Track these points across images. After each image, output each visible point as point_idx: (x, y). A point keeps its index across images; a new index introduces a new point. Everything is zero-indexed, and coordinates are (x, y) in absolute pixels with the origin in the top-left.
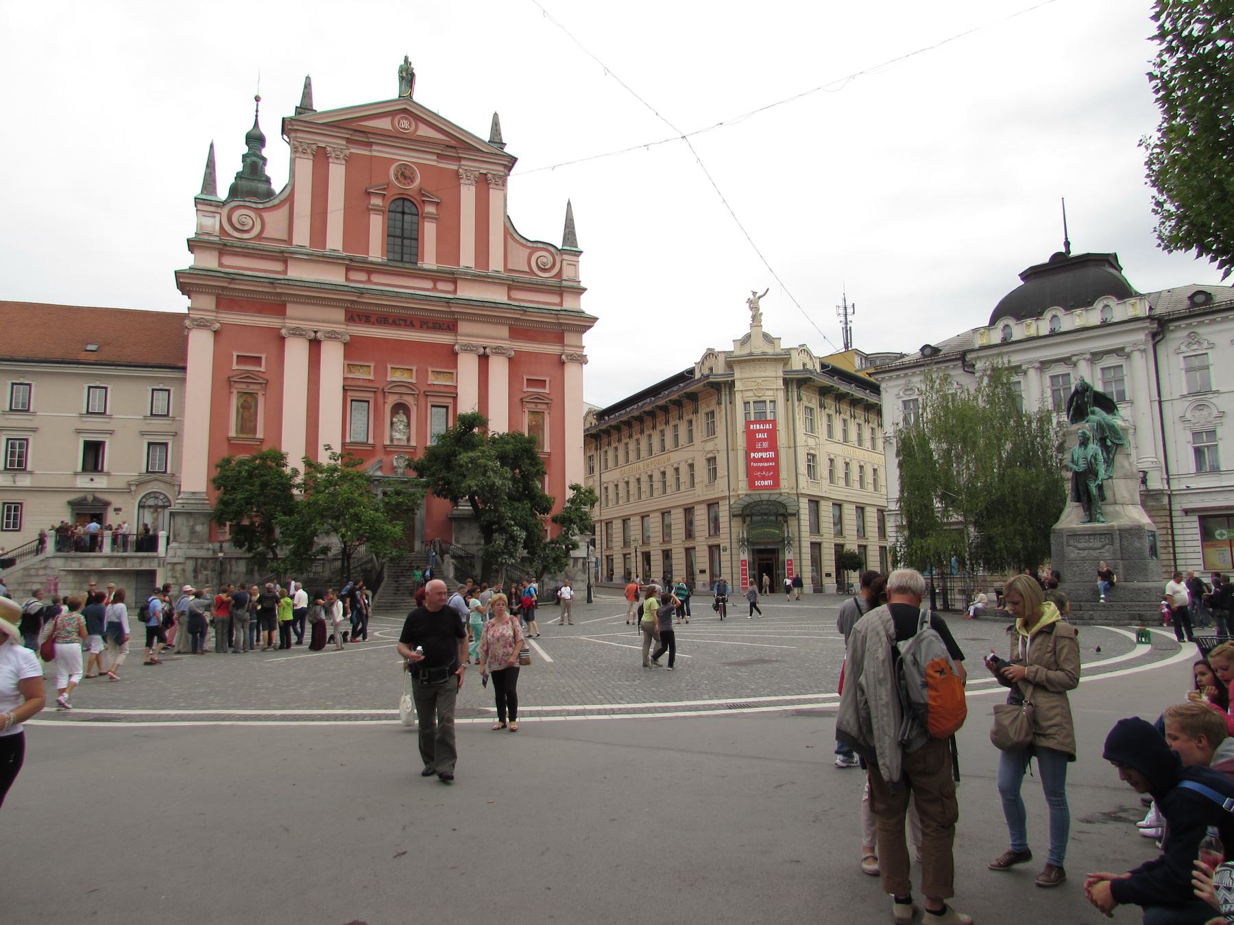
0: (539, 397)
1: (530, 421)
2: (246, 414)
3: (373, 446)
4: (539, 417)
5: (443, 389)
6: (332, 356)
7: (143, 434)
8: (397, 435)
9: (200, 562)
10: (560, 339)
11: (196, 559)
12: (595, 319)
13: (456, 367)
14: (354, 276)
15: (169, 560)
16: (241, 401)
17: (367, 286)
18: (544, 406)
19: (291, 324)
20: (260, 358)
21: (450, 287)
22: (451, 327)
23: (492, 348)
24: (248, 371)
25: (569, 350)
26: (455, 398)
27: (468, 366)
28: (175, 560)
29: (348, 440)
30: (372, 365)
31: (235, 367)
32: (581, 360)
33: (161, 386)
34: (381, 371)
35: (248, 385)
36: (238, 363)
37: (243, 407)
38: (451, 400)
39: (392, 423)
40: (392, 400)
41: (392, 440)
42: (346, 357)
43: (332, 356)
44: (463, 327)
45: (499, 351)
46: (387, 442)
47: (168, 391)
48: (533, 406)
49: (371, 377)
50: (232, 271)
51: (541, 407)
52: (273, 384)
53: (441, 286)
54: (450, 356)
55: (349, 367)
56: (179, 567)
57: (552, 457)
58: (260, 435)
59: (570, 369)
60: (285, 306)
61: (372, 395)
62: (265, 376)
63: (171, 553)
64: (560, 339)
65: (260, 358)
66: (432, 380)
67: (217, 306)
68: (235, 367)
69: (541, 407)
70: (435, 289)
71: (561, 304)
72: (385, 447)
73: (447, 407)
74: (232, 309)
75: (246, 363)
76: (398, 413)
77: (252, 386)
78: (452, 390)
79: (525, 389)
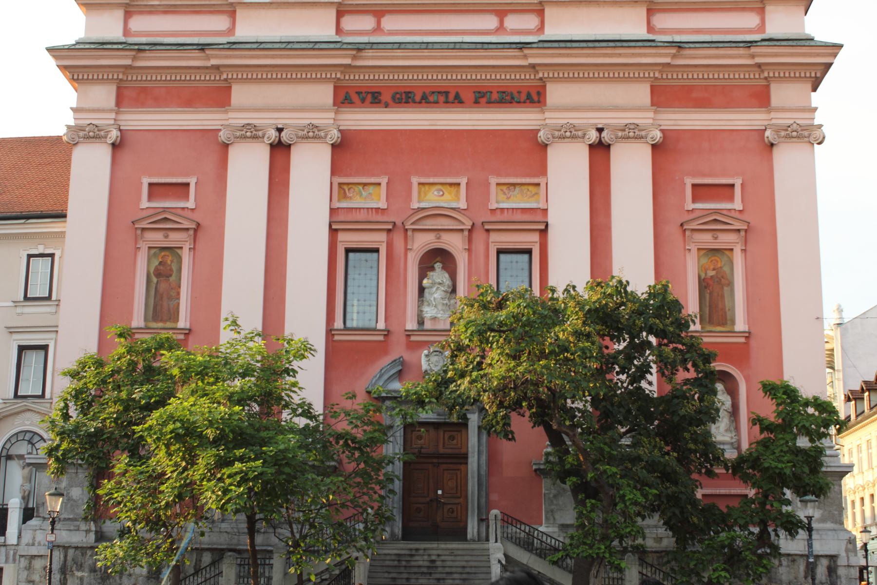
0: (716, 223)
1: (702, 268)
2: (163, 286)
3: (387, 333)
4: (721, 262)
5: (519, 217)
6: (311, 169)
7: (12, 331)
8: (429, 312)
9: (71, 552)
10: (761, 98)
11: (66, 548)
12: (841, 46)
13: (542, 169)
14: (350, 23)
15: (23, 550)
16: (156, 263)
17: (374, 39)
18: (731, 238)
19: (237, 119)
20: (187, 185)
21: (530, 22)
22: (534, 97)
23: (615, 129)
24: (165, 210)
25: (782, 119)
26: (544, 232)
27: (568, 167)
28: (34, 551)
29: (338, 324)
30: (384, 181)
31: (145, 204)
32: (808, 135)
33: (41, 250)
34: (398, 190)
35: (164, 233)
36: (151, 197)
37: (158, 274)
38: (536, 237)
39: (422, 290)
40: (422, 242)
41: (421, 322)
42: (334, 172)
43: (311, 169)
44: (556, 93)
45: (632, 133)
46: (411, 325)
47: (52, 256)
48: (707, 237)
49: (383, 205)
50: (144, 40)
51: (726, 239)
52: (205, 232)
53: (512, 22)
54: (532, 151)
55: (340, 190)
56: (38, 564)
57: (753, 343)
58: (182, 323)
59: (785, 159)
60: (229, 88)
61: (382, 237)
62: (197, 217)
63: (27, 537)
64: (761, 98)
65: (187, 185)
66: (498, 200)
67: (119, 102)
68: (145, 204)
69: (726, 239)
70: (501, 29)
71: (762, 28)
72: (409, 334)
73: (529, 252)
74: (143, 105)
75: (164, 197)
76: (432, 269)
77: (173, 236)
78: (539, 218)
79: (690, 206)
